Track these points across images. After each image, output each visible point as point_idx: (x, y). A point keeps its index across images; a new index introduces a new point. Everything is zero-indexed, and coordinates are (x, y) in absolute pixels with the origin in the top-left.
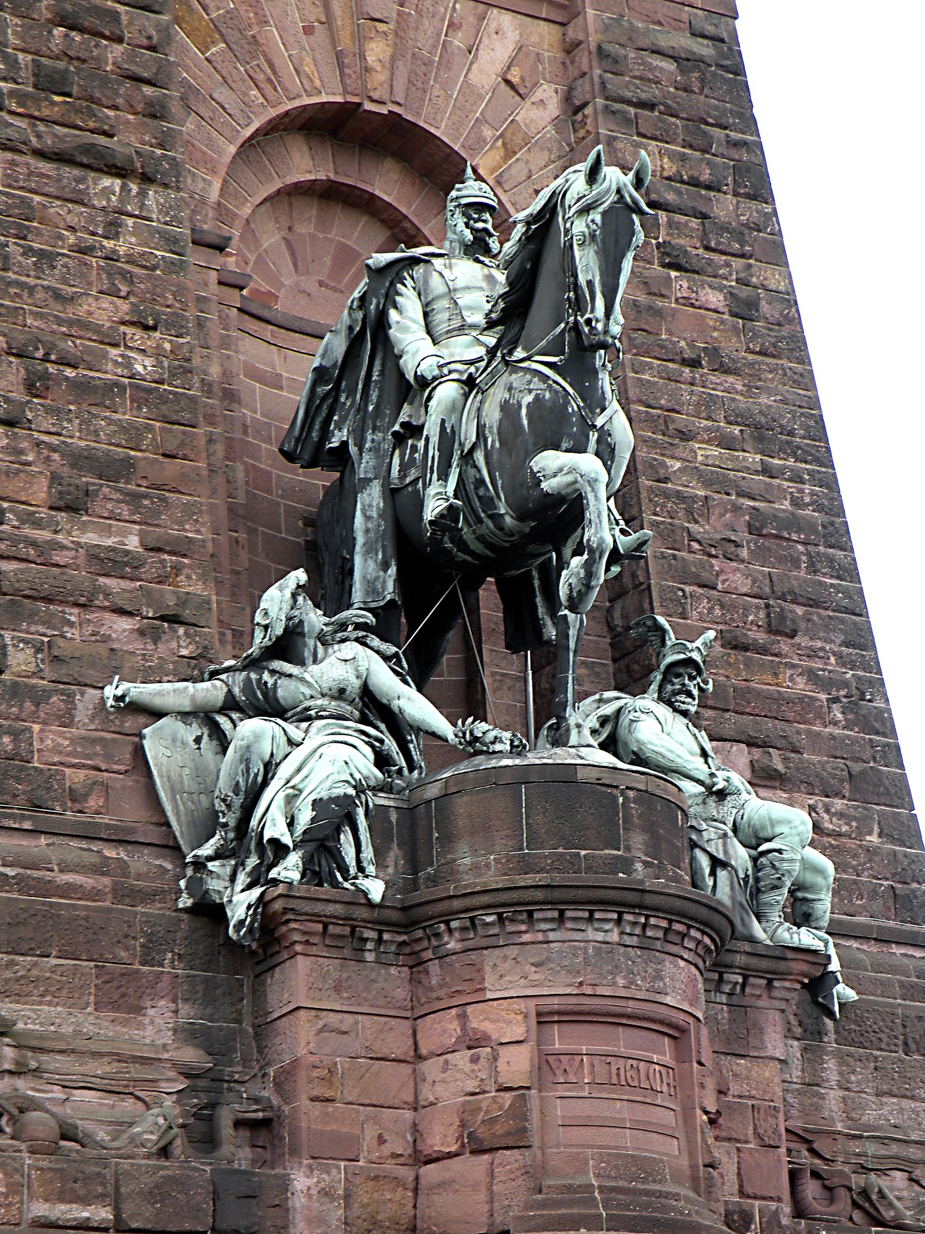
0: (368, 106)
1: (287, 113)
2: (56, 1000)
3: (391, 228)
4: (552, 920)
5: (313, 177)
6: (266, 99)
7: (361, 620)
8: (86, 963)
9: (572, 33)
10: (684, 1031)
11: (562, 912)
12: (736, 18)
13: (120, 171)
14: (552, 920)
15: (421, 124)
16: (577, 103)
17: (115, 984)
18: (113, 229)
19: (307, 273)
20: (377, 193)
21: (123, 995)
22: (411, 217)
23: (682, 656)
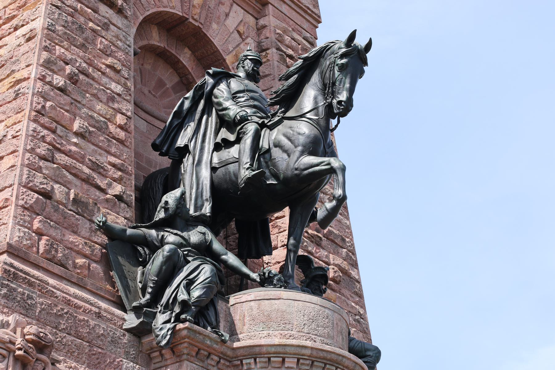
0: (191, 20)
1: (161, 12)
2: (72, 357)
3: (180, 78)
4: (308, 365)
5: (159, 45)
6: (155, 4)
7: (205, 218)
8: (85, 343)
9: (262, 22)
11: (313, 362)
12: (317, 39)
14: (308, 365)
15: (208, 35)
16: (264, 48)
17: (96, 356)
18: (106, 27)
19: (145, 85)
20: (181, 59)
21: (99, 363)
22: (192, 73)
23: (322, 273)
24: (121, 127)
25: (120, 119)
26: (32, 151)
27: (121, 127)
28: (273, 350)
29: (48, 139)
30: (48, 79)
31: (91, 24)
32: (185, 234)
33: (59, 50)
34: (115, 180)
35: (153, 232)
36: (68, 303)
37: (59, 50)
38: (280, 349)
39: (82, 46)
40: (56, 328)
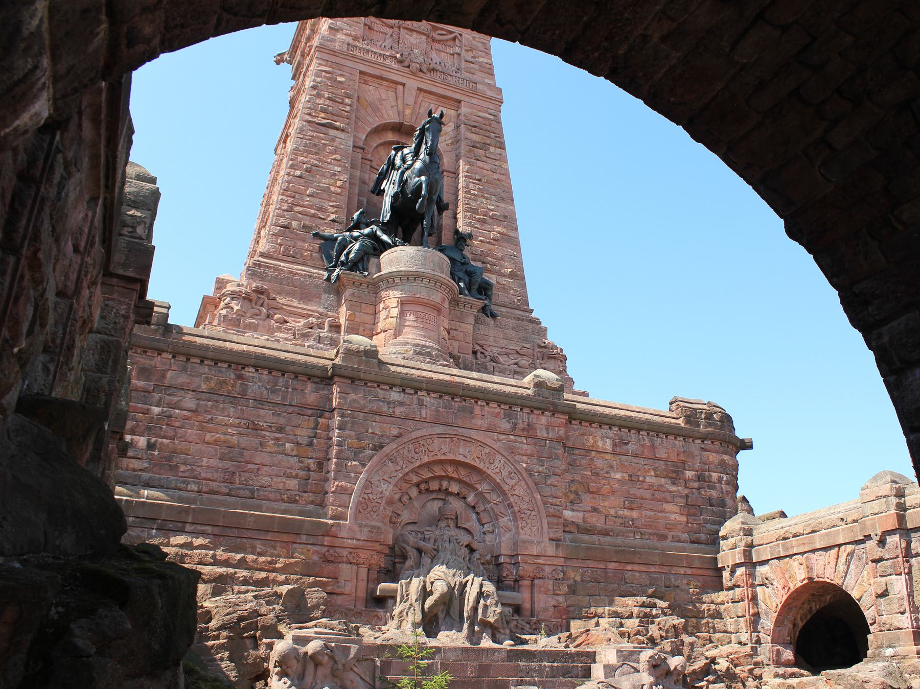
0: (405, 123)
10: (440, 309)
13: (337, 128)
18: (333, 140)
24: (339, 187)
25: (339, 183)
26: (280, 208)
27: (339, 187)
28: (387, 275)
29: (289, 202)
30: (292, 173)
31: (323, 141)
32: (362, 231)
33: (300, 158)
34: (332, 213)
35: (348, 233)
36: (292, 273)
37: (300, 158)
38: (390, 275)
39: (316, 153)
40: (281, 284)
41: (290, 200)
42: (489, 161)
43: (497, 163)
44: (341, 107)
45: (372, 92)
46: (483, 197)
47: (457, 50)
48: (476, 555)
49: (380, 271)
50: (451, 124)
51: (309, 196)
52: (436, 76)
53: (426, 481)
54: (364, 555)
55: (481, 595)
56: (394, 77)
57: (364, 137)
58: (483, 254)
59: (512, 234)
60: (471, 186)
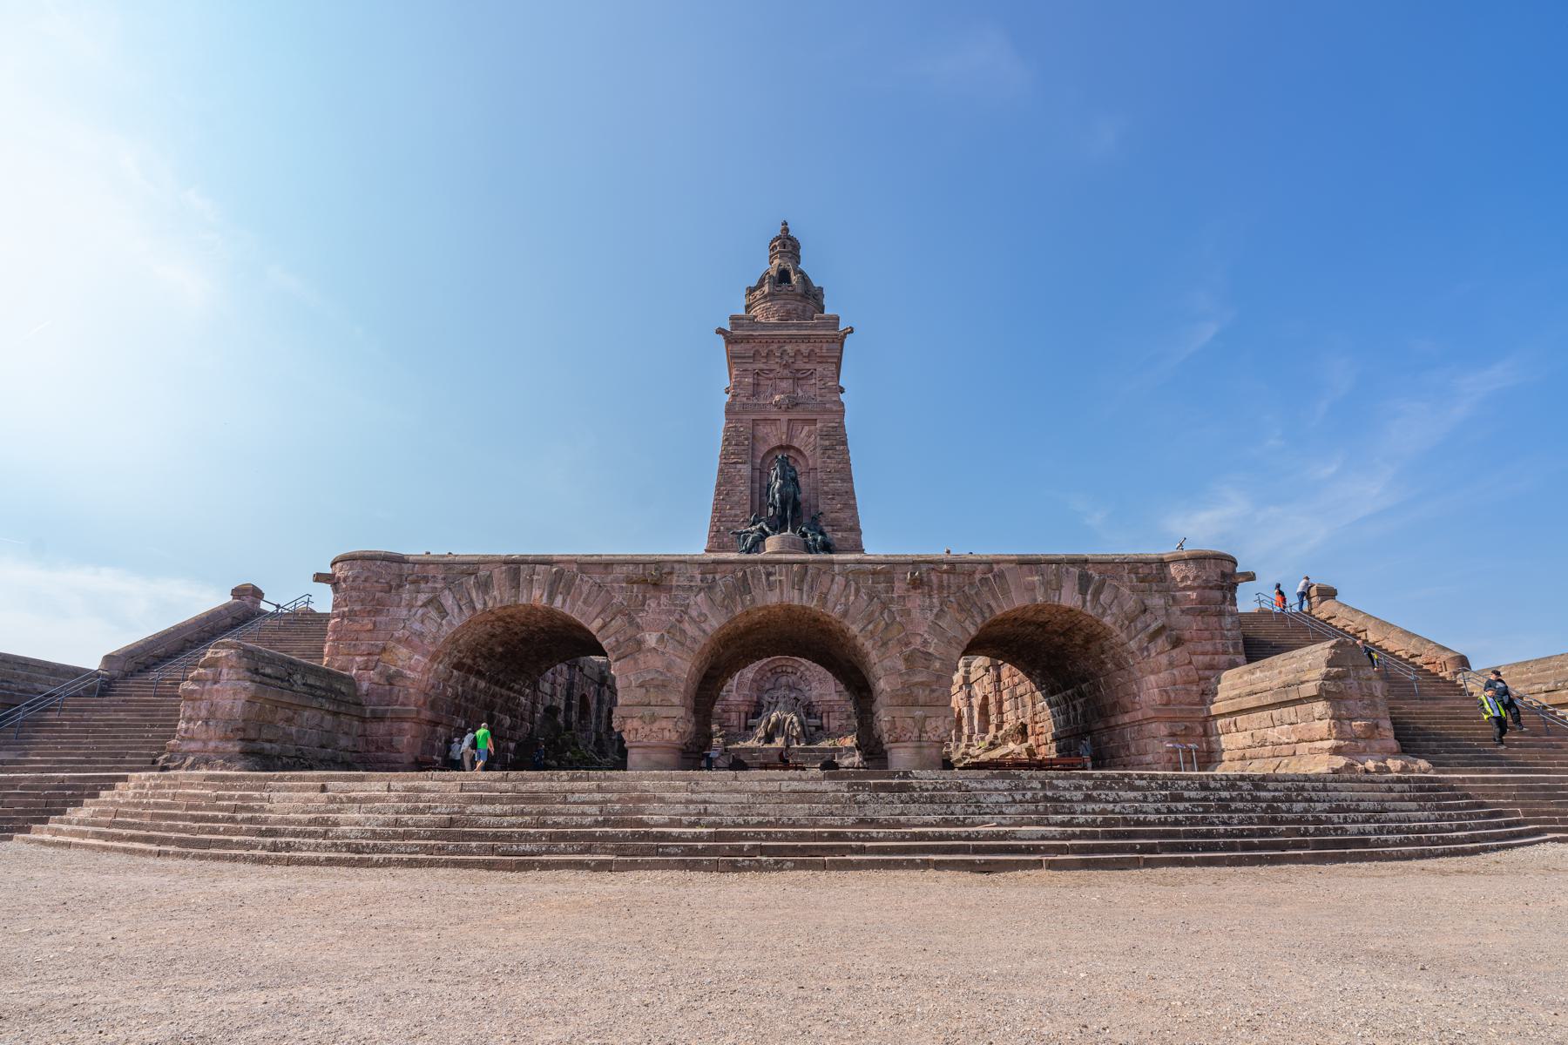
13: (741, 463)
18: (740, 471)
41: (718, 515)
42: (836, 457)
43: (841, 457)
44: (743, 448)
45: (763, 430)
46: (833, 482)
47: (813, 381)
48: (799, 703)
49: (765, 550)
50: (813, 436)
51: (729, 509)
52: (799, 408)
53: (775, 668)
54: (742, 708)
55: (791, 722)
56: (773, 417)
57: (759, 461)
58: (833, 519)
59: (852, 502)
60: (824, 477)
